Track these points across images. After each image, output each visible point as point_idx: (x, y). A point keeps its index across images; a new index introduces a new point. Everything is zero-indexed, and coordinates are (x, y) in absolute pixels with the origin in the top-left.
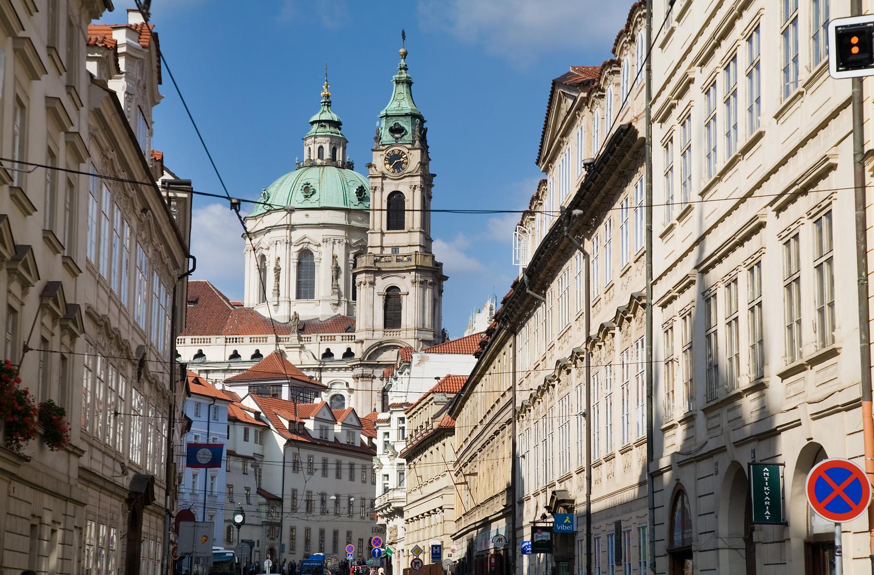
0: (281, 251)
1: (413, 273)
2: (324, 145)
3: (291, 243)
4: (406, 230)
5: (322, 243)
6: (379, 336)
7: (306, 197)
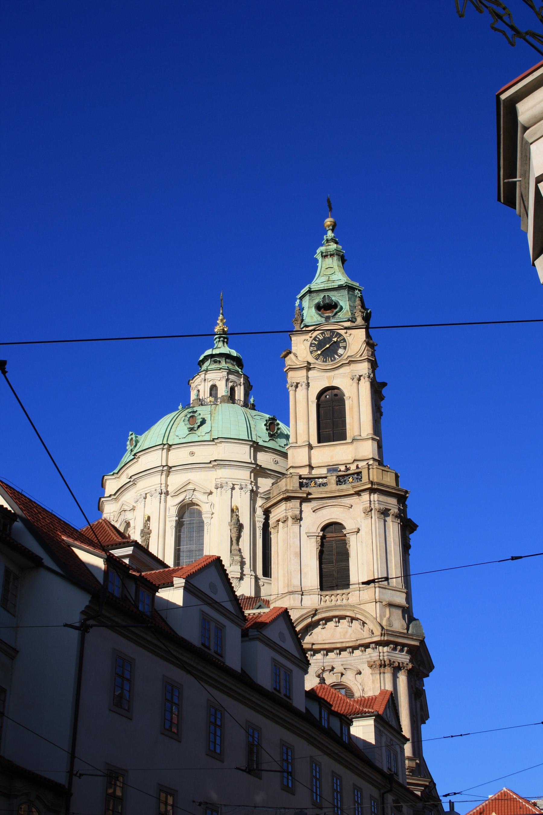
0: (153, 507)
1: (365, 496)
2: (218, 384)
3: (167, 493)
4: (349, 440)
5: (214, 490)
6: (312, 601)
7: (191, 429)
